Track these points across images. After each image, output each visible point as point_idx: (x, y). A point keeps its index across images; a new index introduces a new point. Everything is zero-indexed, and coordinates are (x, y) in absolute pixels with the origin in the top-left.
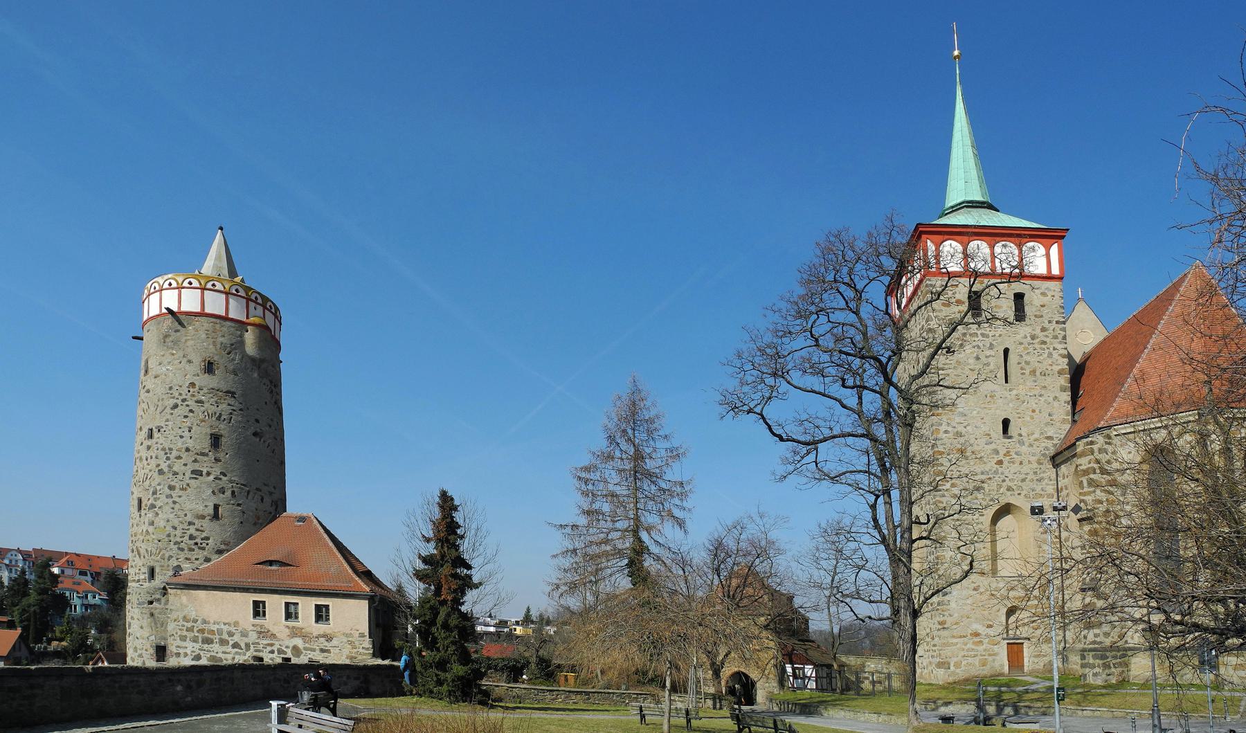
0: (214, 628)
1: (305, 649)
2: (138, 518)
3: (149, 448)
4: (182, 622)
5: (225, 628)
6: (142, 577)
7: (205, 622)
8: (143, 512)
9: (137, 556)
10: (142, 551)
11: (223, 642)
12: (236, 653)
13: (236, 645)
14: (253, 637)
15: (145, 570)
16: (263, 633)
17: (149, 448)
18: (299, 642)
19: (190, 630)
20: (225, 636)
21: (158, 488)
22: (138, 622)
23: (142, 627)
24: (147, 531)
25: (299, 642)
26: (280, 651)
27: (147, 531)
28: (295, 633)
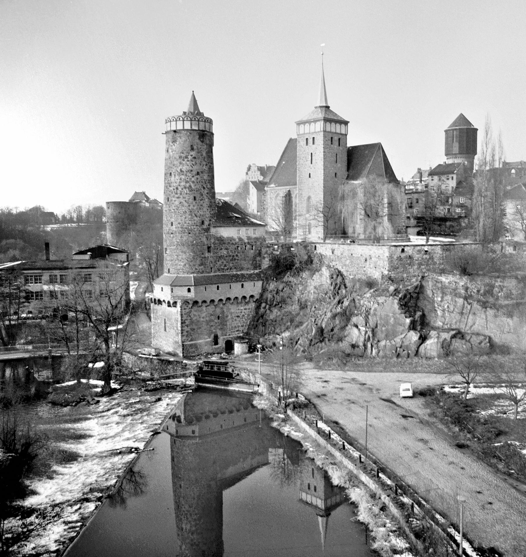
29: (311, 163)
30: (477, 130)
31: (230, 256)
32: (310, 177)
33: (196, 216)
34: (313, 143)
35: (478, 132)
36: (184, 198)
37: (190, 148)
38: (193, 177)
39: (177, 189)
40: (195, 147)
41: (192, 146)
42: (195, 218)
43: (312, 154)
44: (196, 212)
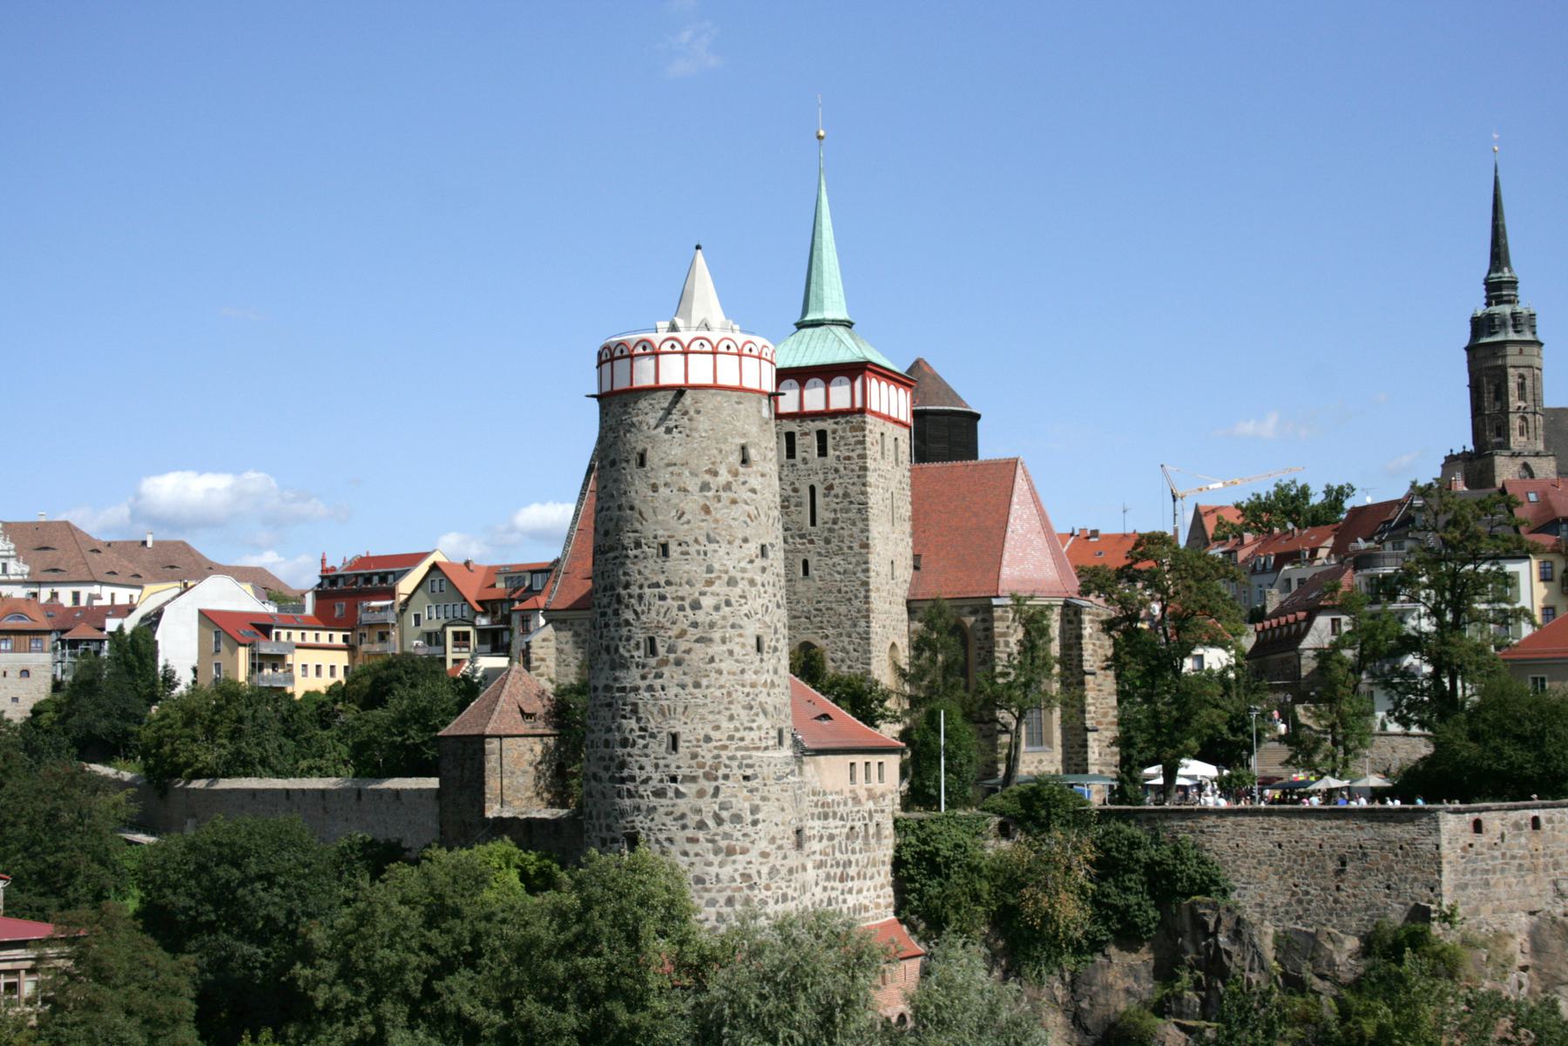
0: (829, 798)
1: (876, 811)
2: (757, 663)
3: (764, 570)
4: (812, 798)
5: (837, 798)
6: (771, 743)
7: (825, 794)
8: (765, 656)
9: (761, 715)
10: (770, 709)
11: (835, 816)
12: (844, 826)
13: (842, 819)
14: (850, 802)
15: (774, 733)
16: (857, 801)
17: (764, 570)
18: (870, 805)
19: (816, 805)
20: (836, 809)
21: (779, 625)
22: (776, 804)
23: (783, 810)
24: (772, 682)
25: (870, 805)
26: (864, 818)
27: (772, 682)
28: (871, 796)
29: (813, 523)
30: (977, 417)
31: (838, 864)
32: (806, 572)
33: (765, 713)
34: (823, 451)
35: (980, 424)
36: (724, 641)
37: (735, 458)
38: (751, 562)
39: (696, 606)
40: (752, 452)
41: (743, 448)
42: (761, 720)
43: (812, 489)
44: (763, 698)
